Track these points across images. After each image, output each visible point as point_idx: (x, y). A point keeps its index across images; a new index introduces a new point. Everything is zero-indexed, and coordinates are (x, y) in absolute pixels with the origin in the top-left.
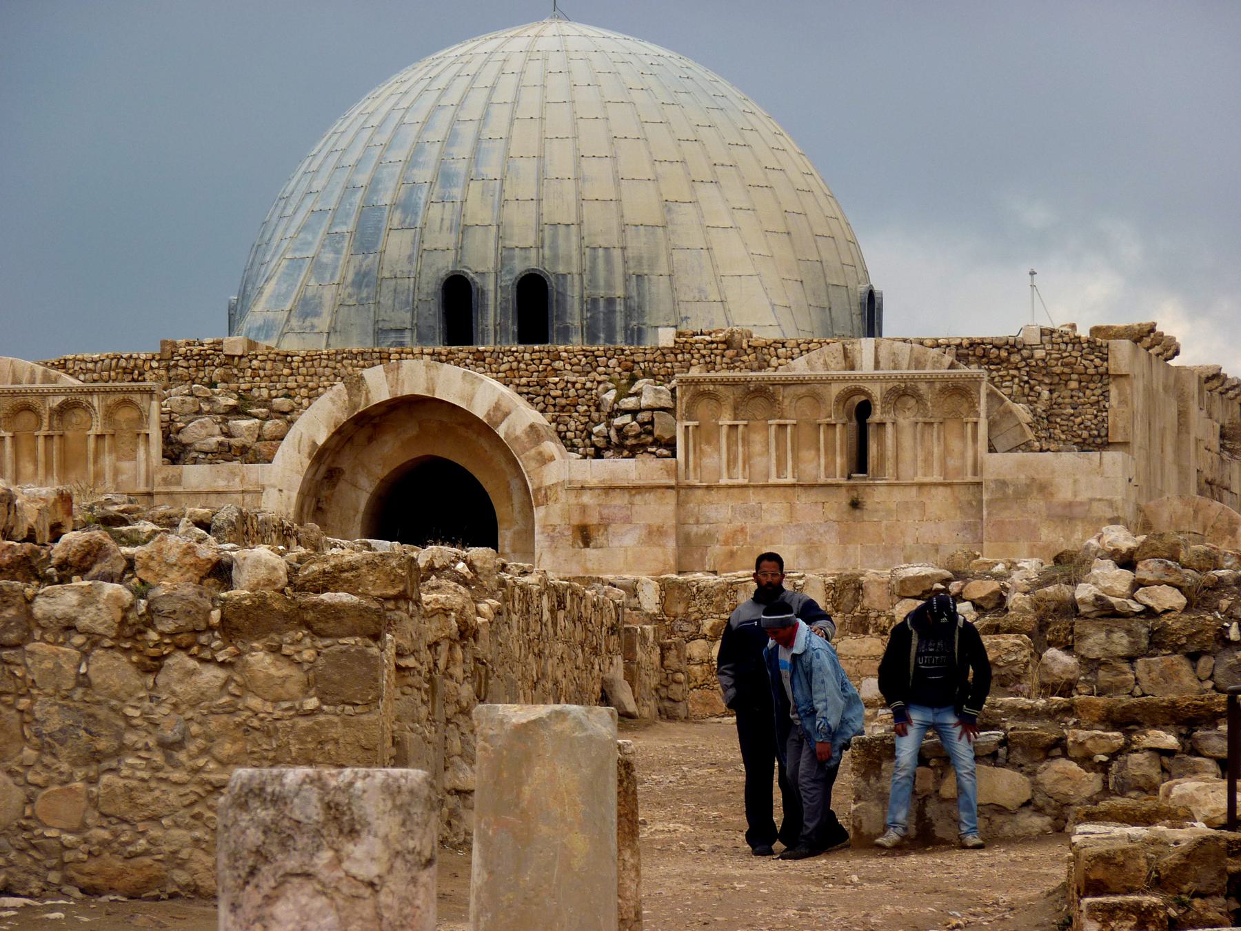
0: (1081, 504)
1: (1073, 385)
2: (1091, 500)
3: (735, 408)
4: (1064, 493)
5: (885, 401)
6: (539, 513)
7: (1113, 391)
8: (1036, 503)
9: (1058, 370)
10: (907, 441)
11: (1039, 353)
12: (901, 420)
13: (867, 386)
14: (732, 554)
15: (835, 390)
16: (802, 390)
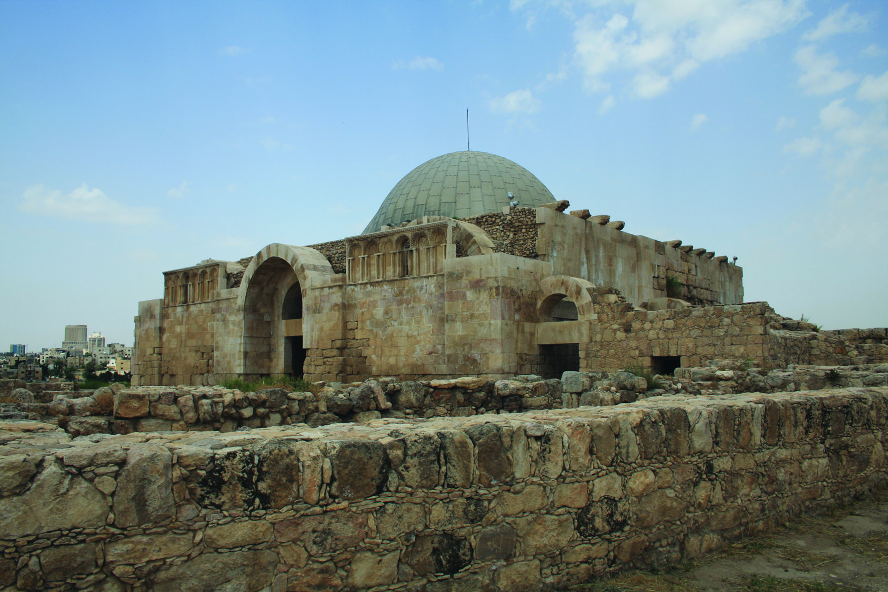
0: (481, 281)
1: (523, 230)
2: (488, 278)
3: (365, 250)
4: (477, 276)
5: (414, 240)
6: (304, 301)
7: (539, 231)
8: (464, 281)
9: (516, 224)
10: (423, 256)
11: (509, 218)
12: (421, 248)
13: (406, 234)
14: (363, 313)
15: (395, 237)
16: (386, 239)
